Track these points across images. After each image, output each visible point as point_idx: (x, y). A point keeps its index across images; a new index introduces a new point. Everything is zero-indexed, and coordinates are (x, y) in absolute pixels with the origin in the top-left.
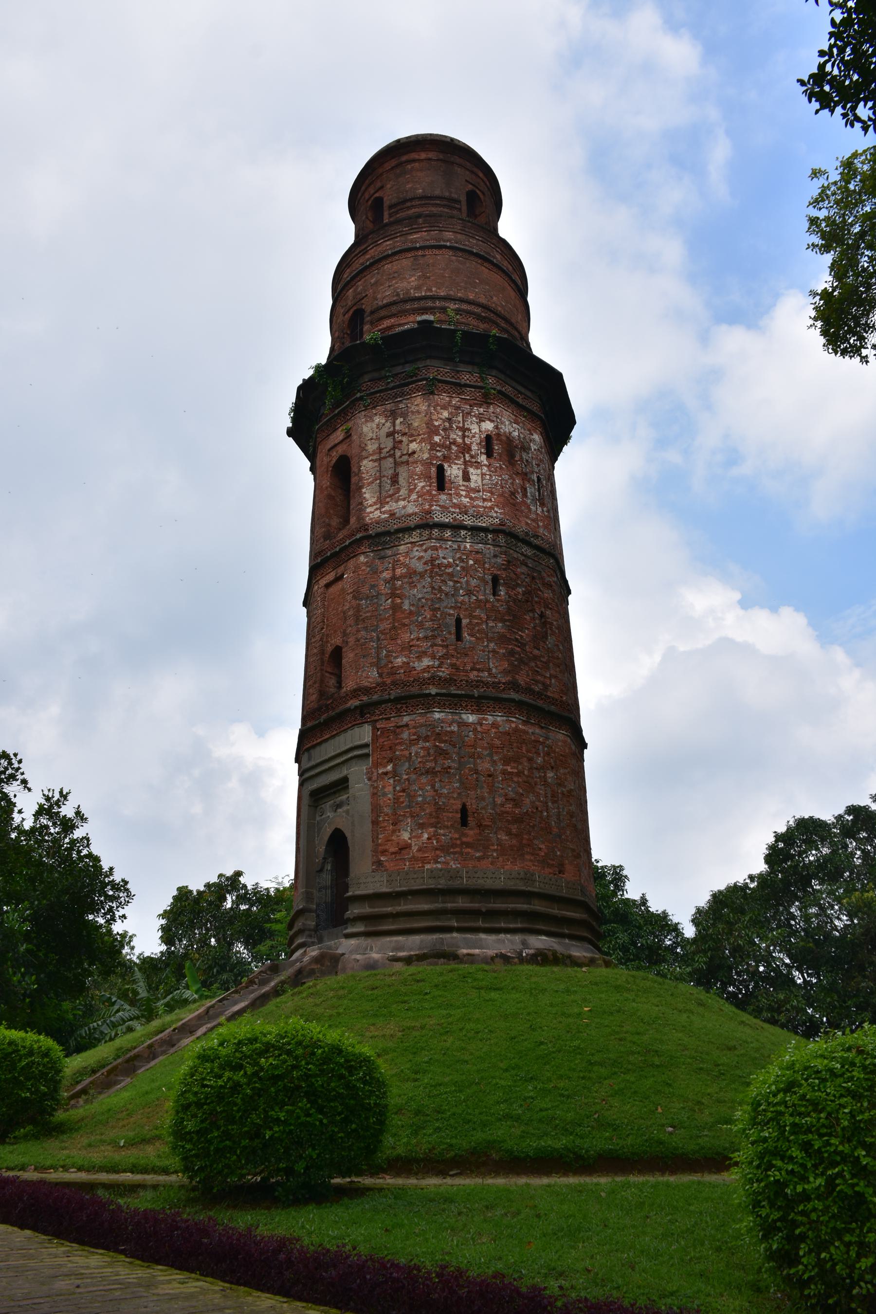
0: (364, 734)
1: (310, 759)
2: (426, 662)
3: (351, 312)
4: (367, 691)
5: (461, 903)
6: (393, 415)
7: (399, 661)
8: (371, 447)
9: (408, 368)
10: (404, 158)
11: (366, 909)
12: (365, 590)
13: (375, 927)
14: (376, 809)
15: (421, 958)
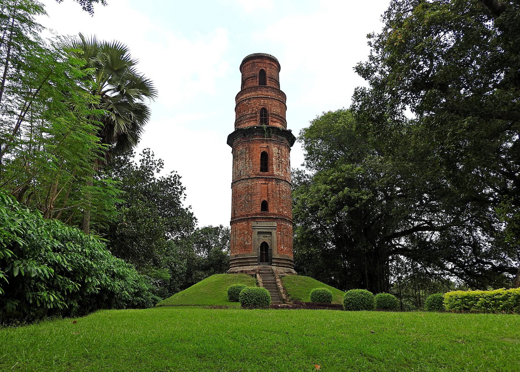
0: (275, 224)
1: (257, 224)
2: (286, 212)
3: (262, 107)
4: (276, 215)
5: (289, 262)
6: (279, 148)
7: (281, 210)
8: (275, 155)
9: (281, 138)
10: (272, 63)
11: (276, 261)
12: (274, 191)
13: (278, 265)
14: (277, 241)
15: (289, 272)
